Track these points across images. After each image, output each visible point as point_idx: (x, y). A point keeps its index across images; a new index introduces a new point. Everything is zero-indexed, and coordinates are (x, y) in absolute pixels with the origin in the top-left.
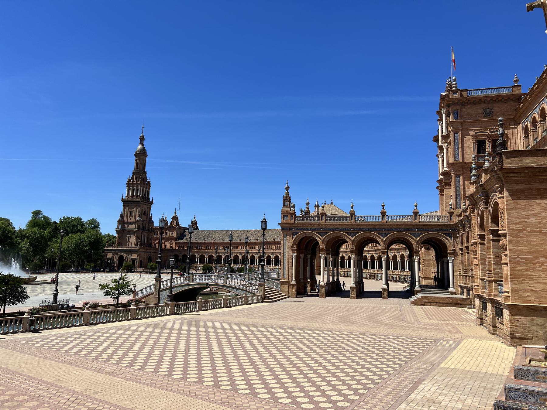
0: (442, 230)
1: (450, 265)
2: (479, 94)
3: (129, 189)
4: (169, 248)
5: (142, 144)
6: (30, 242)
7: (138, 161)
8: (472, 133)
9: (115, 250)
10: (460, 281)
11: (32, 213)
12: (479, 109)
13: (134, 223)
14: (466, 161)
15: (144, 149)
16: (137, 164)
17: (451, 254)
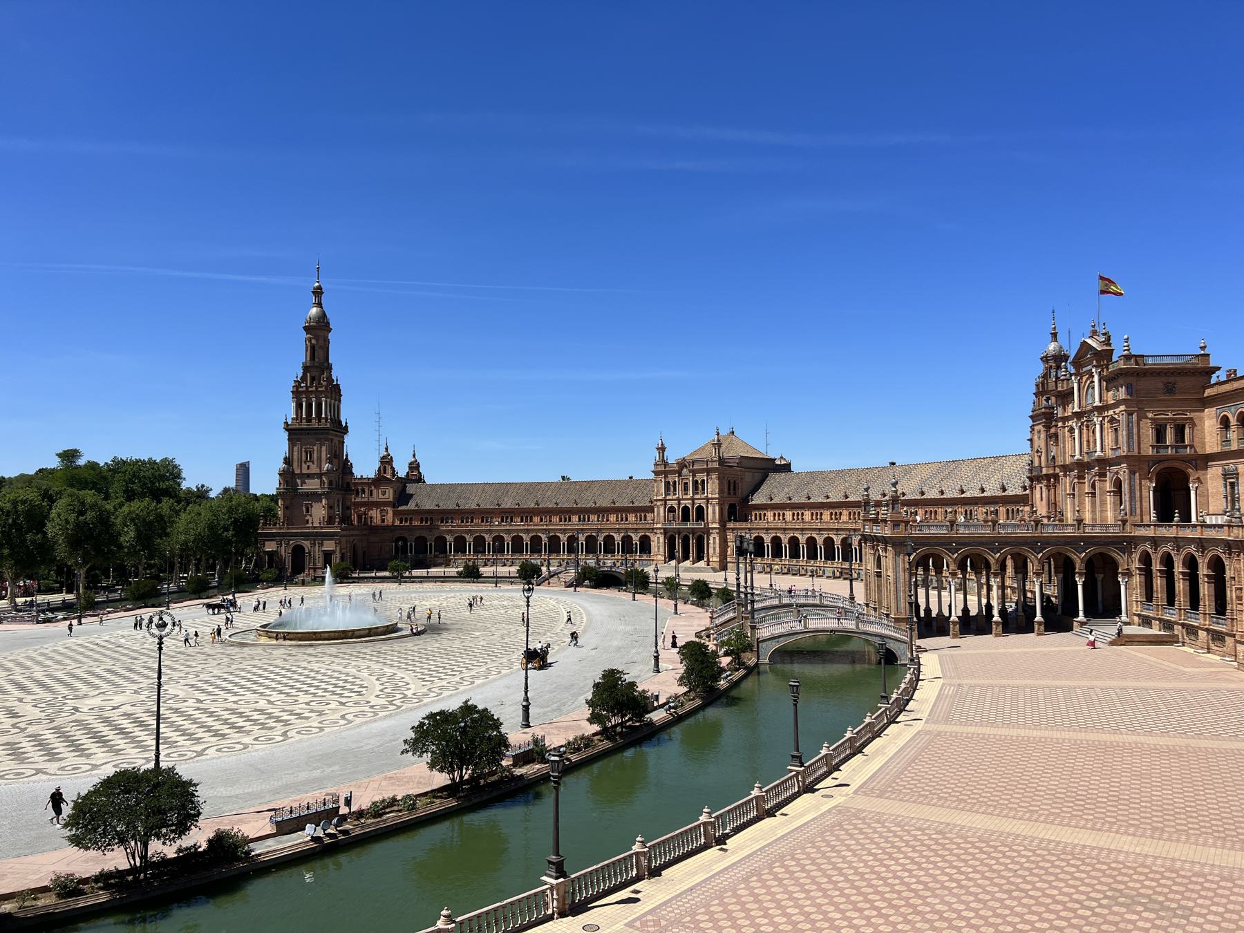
0: (1113, 544)
1: (1123, 588)
2: (1158, 361)
3: (299, 406)
4: (379, 522)
5: (319, 305)
6: (137, 530)
7: (313, 341)
8: (1150, 415)
9: (283, 535)
10: (1136, 608)
11: (59, 455)
12: (1159, 383)
13: (320, 475)
14: (1143, 453)
15: (324, 315)
16: (313, 348)
17: (1123, 574)
